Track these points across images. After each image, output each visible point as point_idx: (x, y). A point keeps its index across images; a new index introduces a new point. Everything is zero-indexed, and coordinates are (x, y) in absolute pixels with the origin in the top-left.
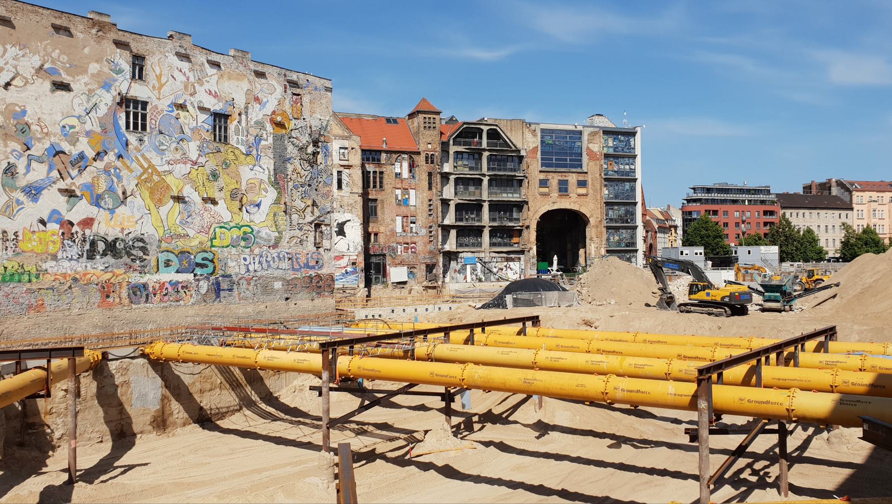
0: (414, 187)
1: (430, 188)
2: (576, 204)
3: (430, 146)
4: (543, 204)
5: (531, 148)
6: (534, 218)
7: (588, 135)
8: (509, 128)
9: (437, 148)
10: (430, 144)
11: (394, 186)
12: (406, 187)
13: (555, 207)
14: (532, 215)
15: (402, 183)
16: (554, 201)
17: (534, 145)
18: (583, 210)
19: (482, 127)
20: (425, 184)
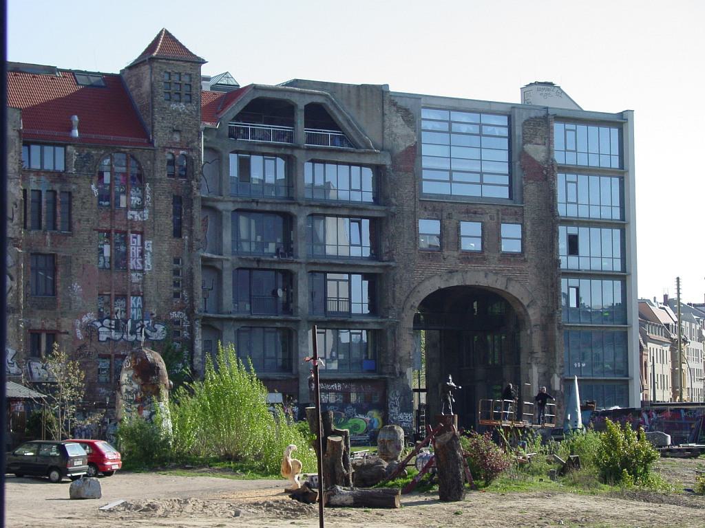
0: (139, 230)
1: (177, 233)
3: (177, 137)
6: (408, 306)
8: (354, 102)
9: (194, 142)
10: (178, 131)
13: (455, 282)
14: (403, 298)
18: (515, 290)
19: (295, 99)
20: (167, 222)
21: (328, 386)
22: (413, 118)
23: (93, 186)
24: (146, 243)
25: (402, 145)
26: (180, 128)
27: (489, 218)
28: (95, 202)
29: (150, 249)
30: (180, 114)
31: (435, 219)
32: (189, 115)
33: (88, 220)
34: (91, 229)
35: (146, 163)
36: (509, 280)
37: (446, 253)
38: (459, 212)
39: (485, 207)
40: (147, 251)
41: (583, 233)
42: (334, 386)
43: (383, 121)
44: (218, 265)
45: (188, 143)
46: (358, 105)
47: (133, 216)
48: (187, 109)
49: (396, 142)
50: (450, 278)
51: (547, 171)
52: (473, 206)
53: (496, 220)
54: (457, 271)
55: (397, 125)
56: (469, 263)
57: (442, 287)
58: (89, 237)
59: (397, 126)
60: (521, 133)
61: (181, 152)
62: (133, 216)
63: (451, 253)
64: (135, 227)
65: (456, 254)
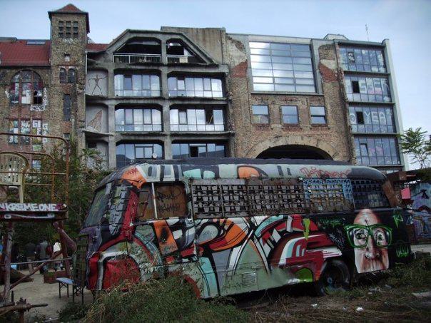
2: (312, 138)
3: (67, 59)
5: (236, 64)
8: (201, 38)
10: (68, 55)
12: (27, 117)
13: (281, 143)
15: (20, 111)
17: (241, 61)
19: (159, 37)
24: (43, 125)
25: (237, 62)
28: (7, 101)
29: (47, 129)
36: (318, 140)
37: (273, 126)
41: (365, 111)
43: (222, 47)
44: (106, 139)
46: (204, 40)
53: (306, 104)
55: (232, 49)
57: (272, 146)
61: (70, 67)
63: (276, 125)
65: (280, 126)
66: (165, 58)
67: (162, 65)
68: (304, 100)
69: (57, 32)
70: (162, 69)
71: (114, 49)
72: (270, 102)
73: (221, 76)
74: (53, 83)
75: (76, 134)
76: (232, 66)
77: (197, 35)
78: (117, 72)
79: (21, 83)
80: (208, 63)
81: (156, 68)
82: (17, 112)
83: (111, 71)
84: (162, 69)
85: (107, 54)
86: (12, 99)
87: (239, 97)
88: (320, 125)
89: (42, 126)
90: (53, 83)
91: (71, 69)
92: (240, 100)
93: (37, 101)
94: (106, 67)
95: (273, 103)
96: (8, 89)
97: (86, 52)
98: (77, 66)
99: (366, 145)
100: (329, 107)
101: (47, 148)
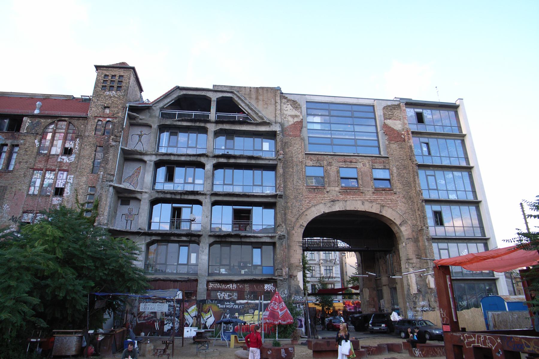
2: (374, 204)
3: (107, 111)
4: (314, 202)
5: (290, 123)
6: (298, 225)
7: (384, 108)
9: (118, 113)
10: (108, 107)
11: (32, 166)
12: (53, 168)
13: (338, 207)
14: (294, 220)
15: (47, 161)
16: (334, 198)
17: (296, 120)
18: (388, 213)
19: (209, 94)
21: (223, 286)
22: (299, 105)
23: (36, 141)
24: (69, 177)
25: (291, 121)
26: (109, 105)
27: (362, 165)
29: (71, 181)
30: (111, 97)
31: (318, 166)
32: (117, 98)
33: (27, 162)
34: (28, 168)
35: (81, 127)
38: (338, 162)
39: (358, 158)
40: (68, 182)
42: (230, 286)
44: (139, 196)
45: (114, 114)
46: (257, 99)
47: (63, 159)
48: (117, 95)
49: (286, 119)
50: (333, 205)
51: (404, 136)
52: (348, 158)
54: (338, 200)
56: (348, 195)
57: (327, 212)
58: (25, 173)
59: (287, 110)
60: (382, 114)
61: (108, 119)
62: (63, 159)
63: (333, 188)
64: (63, 167)
65: (337, 189)
66: (213, 115)
67: (209, 122)
68: (366, 161)
69: (100, 85)
70: (208, 126)
71: (161, 105)
72: (325, 163)
73: (272, 135)
74: (87, 134)
75: (102, 188)
76: (286, 125)
77: (250, 94)
78: (162, 128)
79: (54, 133)
80: (259, 121)
81: (202, 125)
82: (43, 163)
83: (155, 126)
84: (208, 126)
85: (153, 110)
86: (39, 148)
87: (292, 157)
88: (384, 190)
89: (67, 179)
90: (87, 134)
91: (109, 121)
92: (292, 160)
93: (67, 152)
94: (150, 123)
95: (330, 164)
96: (39, 137)
97: (128, 105)
98: (116, 118)
99: (427, 144)
100: (395, 170)
101: (68, 202)
